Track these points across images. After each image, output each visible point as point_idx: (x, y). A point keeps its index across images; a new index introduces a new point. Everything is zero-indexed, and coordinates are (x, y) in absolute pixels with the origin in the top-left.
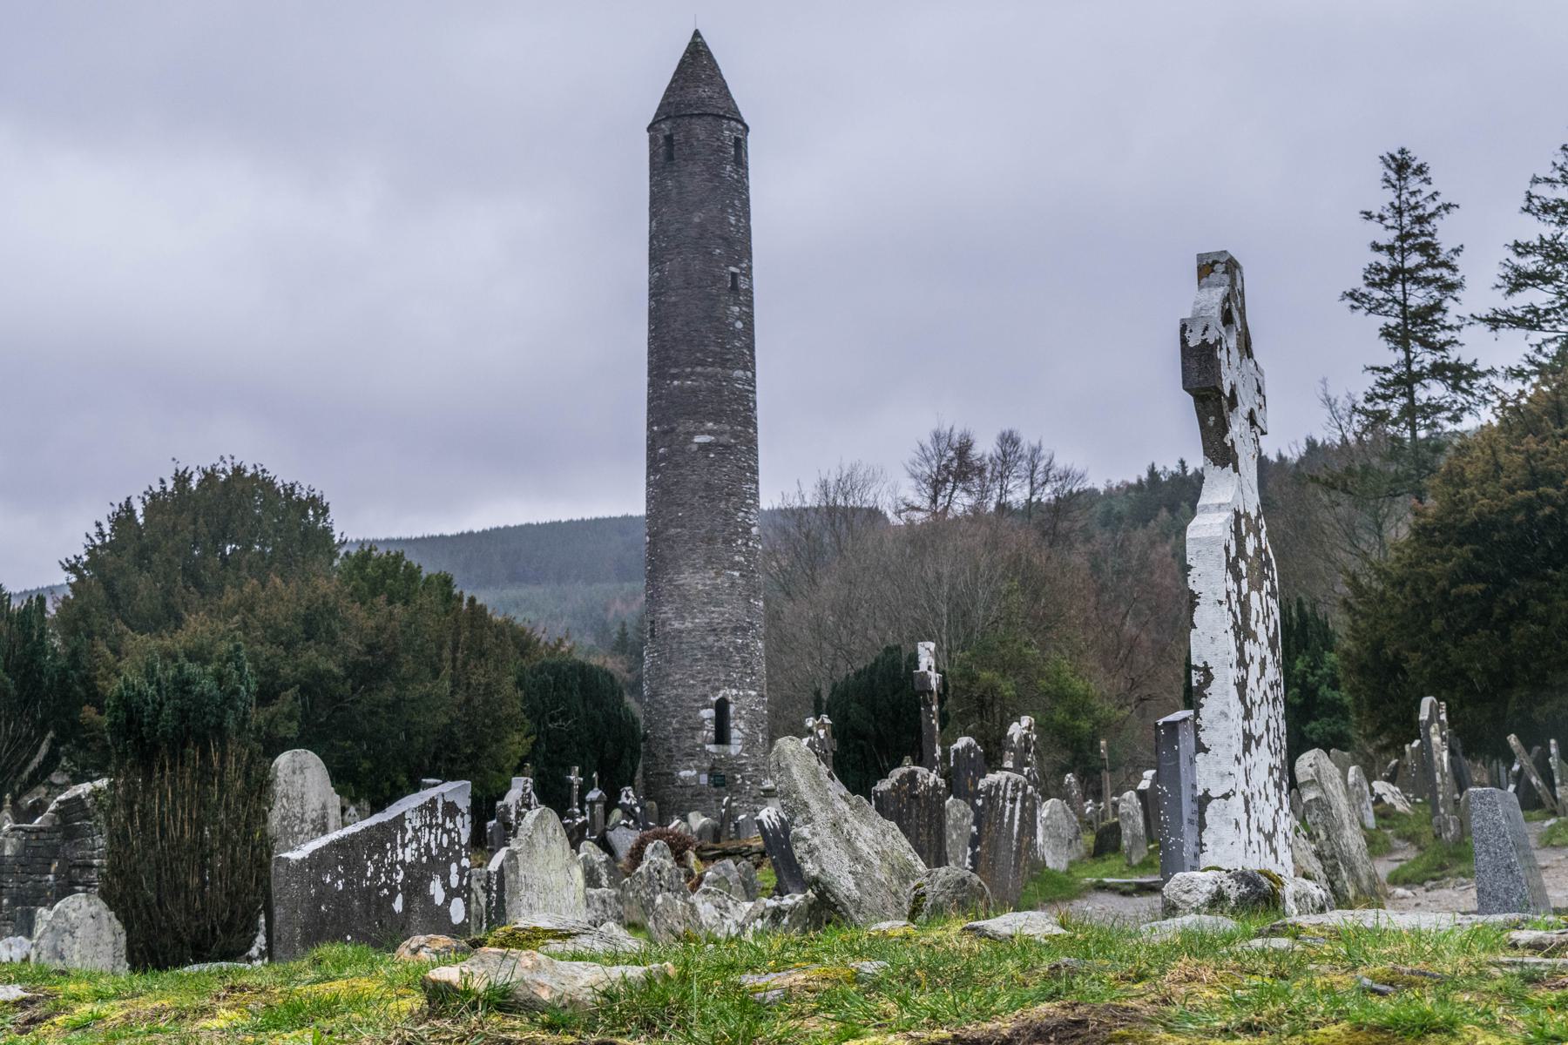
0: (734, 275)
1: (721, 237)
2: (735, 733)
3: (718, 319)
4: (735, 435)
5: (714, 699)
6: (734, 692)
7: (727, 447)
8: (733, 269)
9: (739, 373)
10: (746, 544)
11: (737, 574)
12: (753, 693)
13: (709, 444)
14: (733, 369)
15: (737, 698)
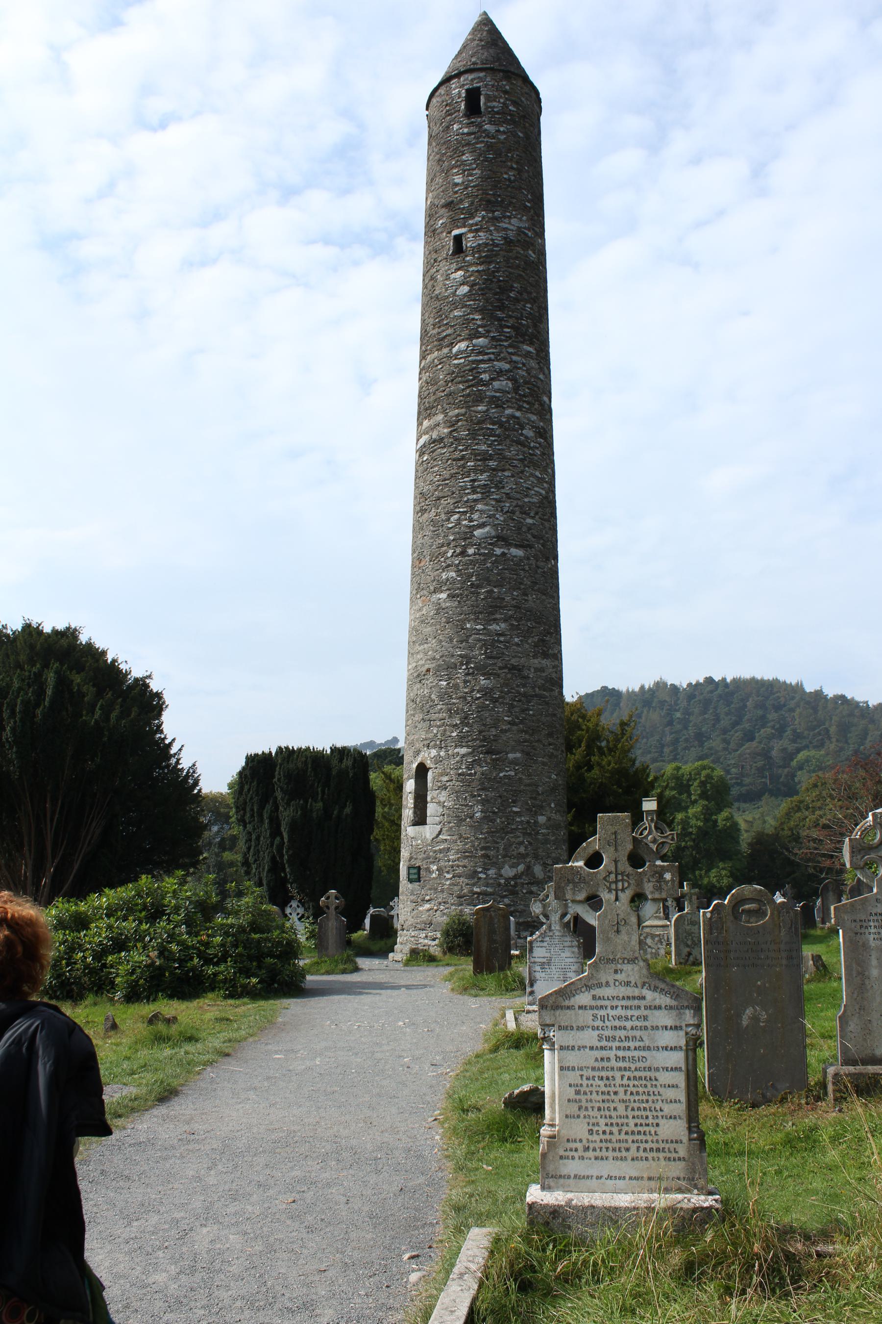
0: (458, 239)
1: (443, 207)
2: (431, 808)
3: (437, 298)
4: (452, 424)
5: (415, 766)
6: (434, 752)
7: (441, 440)
8: (456, 232)
9: (463, 345)
10: (463, 553)
11: (443, 596)
12: (463, 751)
13: (424, 446)
14: (451, 345)
15: (437, 760)
